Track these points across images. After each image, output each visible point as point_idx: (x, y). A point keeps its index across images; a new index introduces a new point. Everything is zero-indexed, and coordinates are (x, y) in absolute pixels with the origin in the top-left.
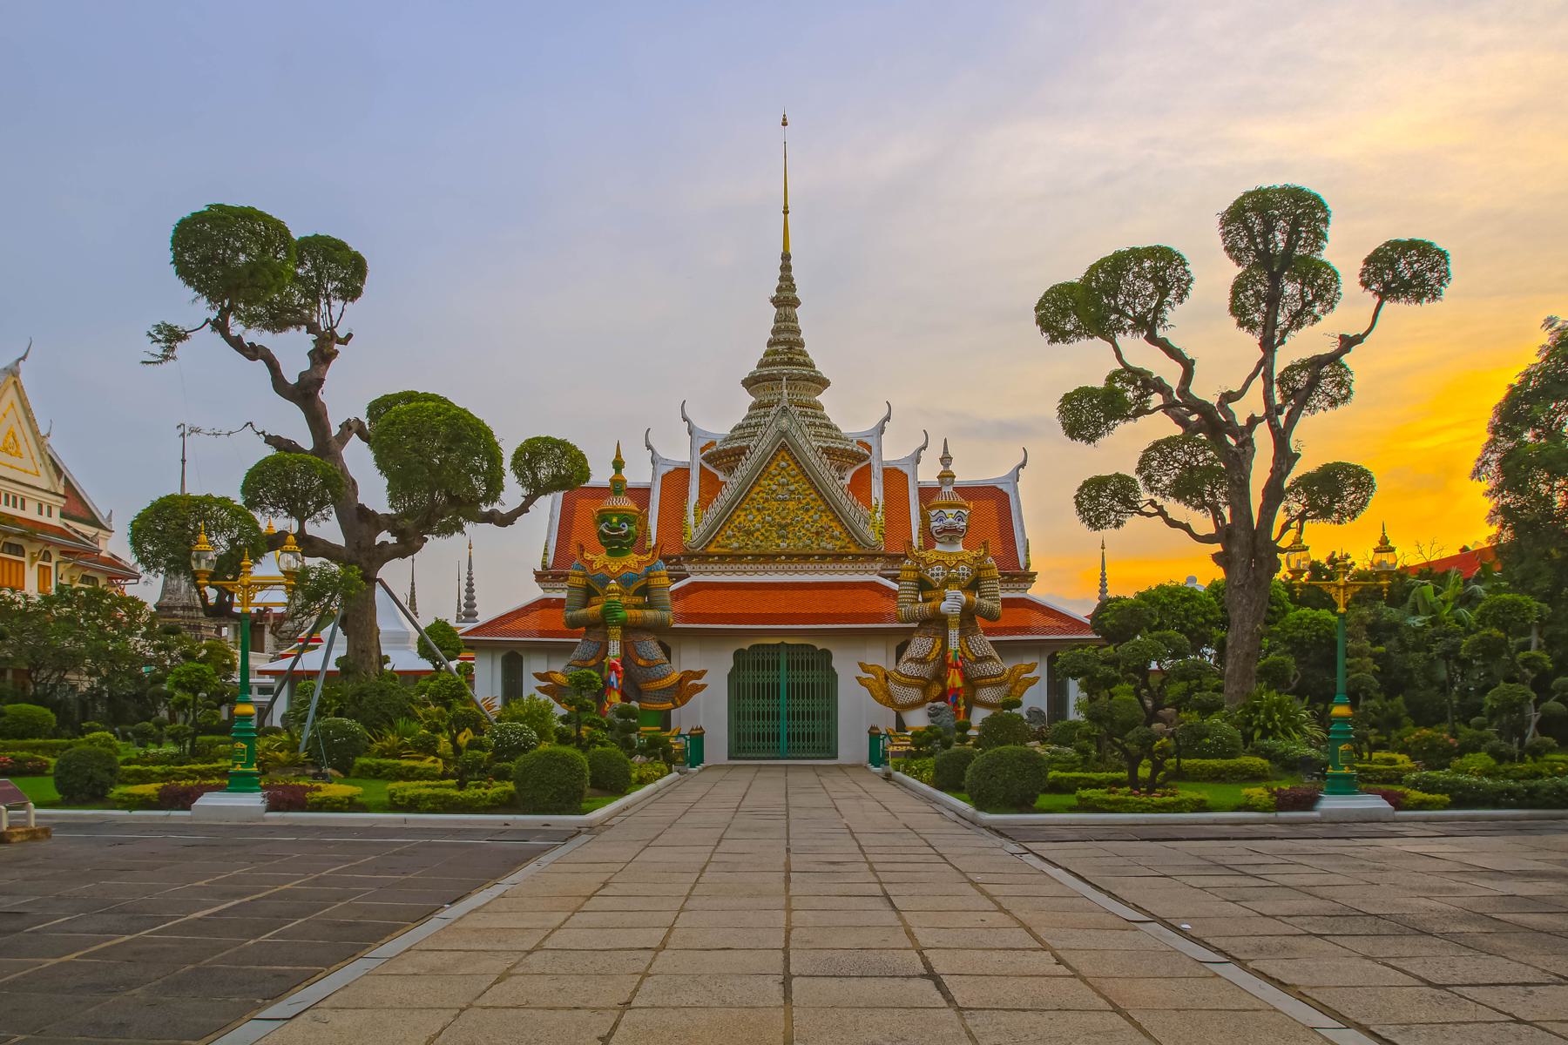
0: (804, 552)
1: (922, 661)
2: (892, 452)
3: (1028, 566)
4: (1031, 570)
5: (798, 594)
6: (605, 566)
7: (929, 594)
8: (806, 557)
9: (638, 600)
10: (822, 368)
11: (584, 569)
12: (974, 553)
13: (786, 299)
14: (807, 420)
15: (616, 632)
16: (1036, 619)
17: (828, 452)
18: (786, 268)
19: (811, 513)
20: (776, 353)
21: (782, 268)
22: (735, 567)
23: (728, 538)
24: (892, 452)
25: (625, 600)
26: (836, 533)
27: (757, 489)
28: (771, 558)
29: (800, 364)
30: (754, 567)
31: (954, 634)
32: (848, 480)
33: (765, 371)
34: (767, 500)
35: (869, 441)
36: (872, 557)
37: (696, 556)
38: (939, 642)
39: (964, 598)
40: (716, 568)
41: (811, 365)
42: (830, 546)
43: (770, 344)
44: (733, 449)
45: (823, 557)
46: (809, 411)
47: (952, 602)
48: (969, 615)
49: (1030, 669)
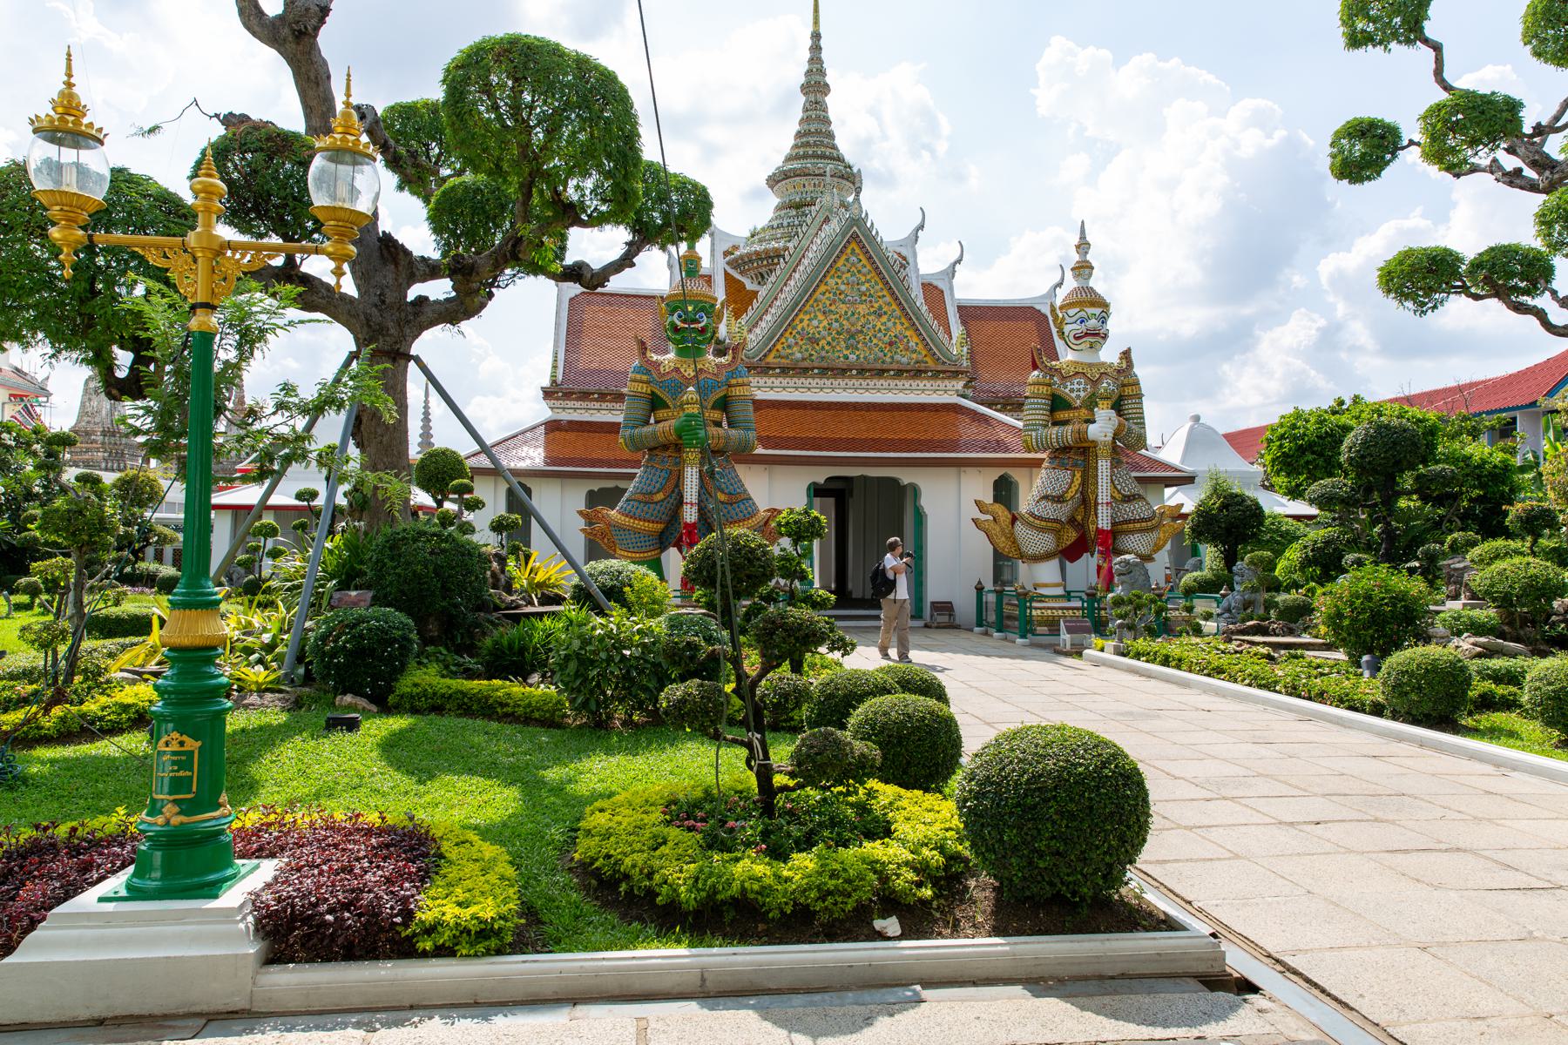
0: (878, 366)
1: (1059, 499)
2: (928, 263)
5: (874, 415)
6: (677, 370)
7: (1062, 415)
8: (881, 373)
9: (716, 415)
11: (648, 372)
13: (815, 86)
15: (692, 455)
18: (816, 48)
19: (884, 319)
20: (807, 144)
22: (799, 381)
24: (928, 263)
27: (823, 288)
28: (842, 372)
30: (821, 382)
31: (1104, 466)
33: (796, 165)
36: (955, 374)
38: (1078, 475)
40: (777, 382)
42: (904, 360)
43: (799, 135)
44: (766, 251)
45: (899, 373)
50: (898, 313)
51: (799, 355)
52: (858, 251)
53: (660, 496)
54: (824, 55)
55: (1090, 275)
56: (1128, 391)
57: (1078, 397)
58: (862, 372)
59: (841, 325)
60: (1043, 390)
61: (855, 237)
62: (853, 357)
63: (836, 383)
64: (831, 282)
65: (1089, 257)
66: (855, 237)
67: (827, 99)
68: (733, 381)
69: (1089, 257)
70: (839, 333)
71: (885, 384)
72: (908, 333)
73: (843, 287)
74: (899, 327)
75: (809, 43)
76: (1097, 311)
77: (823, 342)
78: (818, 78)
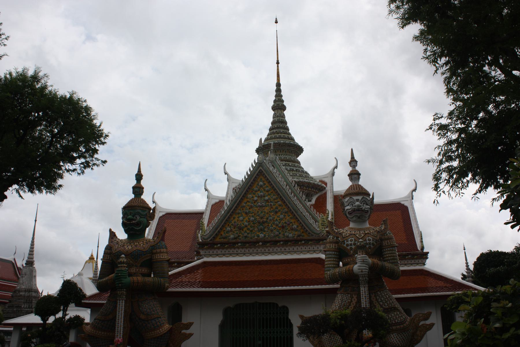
0: (274, 239)
3: (423, 248)
4: (425, 251)
9: (145, 270)
10: (299, 140)
12: (377, 229)
13: (279, 106)
14: (288, 168)
16: (432, 283)
17: (300, 184)
18: (278, 90)
19: (279, 214)
20: (273, 133)
21: (276, 91)
22: (231, 251)
25: (133, 270)
26: (295, 226)
27: (245, 200)
30: (243, 250)
31: (364, 290)
32: (313, 201)
34: (251, 207)
35: (326, 180)
38: (355, 297)
39: (370, 261)
40: (219, 252)
41: (293, 139)
42: (291, 235)
43: (271, 129)
46: (290, 164)
47: (360, 264)
48: (377, 276)
49: (427, 317)
50: (286, 210)
51: (232, 236)
52: (263, 179)
55: (359, 178)
56: (385, 243)
57: (351, 249)
60: (333, 246)
61: (261, 172)
62: (262, 235)
63: (251, 250)
64: (250, 196)
65: (357, 168)
66: (261, 172)
67: (285, 112)
68: (154, 251)
69: (357, 168)
70: (254, 224)
71: (279, 249)
72: (292, 221)
73: (256, 198)
74: (288, 218)
75: (275, 88)
76: (360, 198)
77: (245, 229)
78: (278, 103)
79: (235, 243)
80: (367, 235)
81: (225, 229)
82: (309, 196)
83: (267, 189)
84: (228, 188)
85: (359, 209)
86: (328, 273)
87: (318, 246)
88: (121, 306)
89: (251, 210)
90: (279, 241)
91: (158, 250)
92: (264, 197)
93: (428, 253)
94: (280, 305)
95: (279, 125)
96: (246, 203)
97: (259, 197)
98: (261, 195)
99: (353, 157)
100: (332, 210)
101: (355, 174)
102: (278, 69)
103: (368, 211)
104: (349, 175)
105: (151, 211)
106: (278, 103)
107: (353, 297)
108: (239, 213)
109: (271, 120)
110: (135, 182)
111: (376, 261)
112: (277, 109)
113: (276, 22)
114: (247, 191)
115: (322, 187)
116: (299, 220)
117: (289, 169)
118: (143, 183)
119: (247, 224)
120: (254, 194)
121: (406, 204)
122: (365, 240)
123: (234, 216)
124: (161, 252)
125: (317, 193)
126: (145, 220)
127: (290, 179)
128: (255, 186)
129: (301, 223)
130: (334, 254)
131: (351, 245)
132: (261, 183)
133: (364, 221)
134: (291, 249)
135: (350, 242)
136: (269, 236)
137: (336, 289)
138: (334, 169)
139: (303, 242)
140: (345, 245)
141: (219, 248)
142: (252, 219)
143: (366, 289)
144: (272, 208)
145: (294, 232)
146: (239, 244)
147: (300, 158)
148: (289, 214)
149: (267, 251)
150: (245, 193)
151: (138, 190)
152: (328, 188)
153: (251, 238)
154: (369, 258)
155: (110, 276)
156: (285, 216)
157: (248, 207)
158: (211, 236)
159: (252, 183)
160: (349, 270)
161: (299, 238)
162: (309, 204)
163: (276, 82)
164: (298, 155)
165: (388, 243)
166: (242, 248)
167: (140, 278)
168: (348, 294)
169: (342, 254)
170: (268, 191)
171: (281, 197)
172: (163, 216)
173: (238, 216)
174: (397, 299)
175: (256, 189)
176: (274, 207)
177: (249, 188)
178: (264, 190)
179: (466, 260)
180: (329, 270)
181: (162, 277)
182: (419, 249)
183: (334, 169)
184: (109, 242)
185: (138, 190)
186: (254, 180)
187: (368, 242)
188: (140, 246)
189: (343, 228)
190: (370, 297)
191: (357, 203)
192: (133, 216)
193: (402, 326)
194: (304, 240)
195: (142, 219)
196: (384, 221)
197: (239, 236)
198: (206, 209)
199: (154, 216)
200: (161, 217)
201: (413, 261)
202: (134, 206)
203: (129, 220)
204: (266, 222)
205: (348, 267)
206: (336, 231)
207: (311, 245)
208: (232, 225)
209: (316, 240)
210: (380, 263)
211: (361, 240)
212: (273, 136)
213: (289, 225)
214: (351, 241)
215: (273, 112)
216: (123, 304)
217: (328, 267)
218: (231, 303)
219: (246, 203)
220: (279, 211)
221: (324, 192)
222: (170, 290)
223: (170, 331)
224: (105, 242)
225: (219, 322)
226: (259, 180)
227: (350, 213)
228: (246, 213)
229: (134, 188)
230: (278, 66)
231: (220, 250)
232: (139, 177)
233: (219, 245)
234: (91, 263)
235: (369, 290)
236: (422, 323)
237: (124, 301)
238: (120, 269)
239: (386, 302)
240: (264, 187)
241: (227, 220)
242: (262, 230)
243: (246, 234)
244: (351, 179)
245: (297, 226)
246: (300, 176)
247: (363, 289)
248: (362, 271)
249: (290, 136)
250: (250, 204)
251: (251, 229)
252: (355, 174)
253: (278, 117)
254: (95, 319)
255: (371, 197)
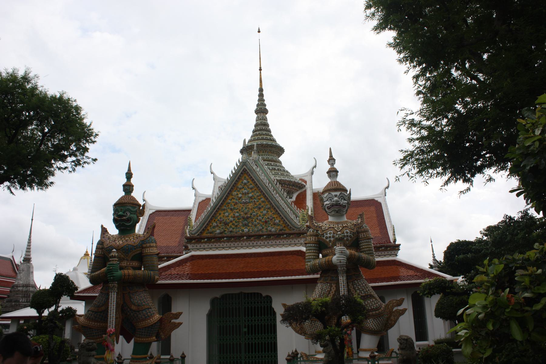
0: (258, 233)
4: (397, 243)
7: (325, 252)
8: (258, 237)
9: (135, 264)
10: (280, 142)
12: (354, 222)
13: (261, 110)
16: (403, 272)
17: (281, 182)
18: (261, 95)
19: (262, 210)
20: (257, 135)
23: (214, 227)
25: (124, 264)
26: (277, 221)
27: (230, 197)
29: (268, 140)
31: (342, 279)
32: (294, 198)
34: (236, 203)
35: (305, 178)
37: (194, 239)
38: (334, 286)
39: (348, 252)
40: (206, 246)
41: (274, 140)
42: (273, 230)
43: (254, 132)
46: (272, 163)
48: (354, 266)
49: (400, 303)
50: (269, 206)
51: (218, 231)
52: (247, 178)
53: (103, 308)
54: (264, 98)
55: (337, 175)
56: (362, 235)
57: (330, 241)
58: (249, 237)
59: (240, 215)
60: (313, 239)
61: (245, 170)
62: (246, 230)
63: (236, 244)
65: (335, 166)
66: (245, 170)
67: (267, 116)
68: (145, 246)
69: (335, 166)
71: (262, 243)
72: (275, 216)
73: (240, 195)
74: (270, 213)
75: (258, 93)
76: (338, 193)
78: (260, 107)
79: (221, 238)
80: (345, 228)
81: (211, 224)
82: (290, 194)
83: (251, 186)
84: (214, 187)
85: (337, 204)
86: (309, 264)
87: (299, 239)
88: (113, 298)
89: (236, 206)
90: (263, 235)
91: (148, 245)
92: (248, 194)
93: (399, 245)
94: (264, 295)
95: (262, 127)
96: (231, 200)
97: (243, 194)
98: (245, 193)
99: (331, 156)
100: (312, 206)
101: (333, 171)
102: (260, 76)
103: (345, 206)
104: (328, 173)
105: (141, 208)
106: (260, 107)
107: (331, 286)
108: (224, 210)
109: (254, 122)
110: (125, 181)
111: (353, 252)
112: (259, 112)
113: (259, 32)
114: (232, 188)
115: (302, 185)
116: (280, 216)
117: (271, 168)
118: (133, 181)
119: (232, 219)
120: (239, 191)
121: (380, 200)
122: (343, 233)
123: (220, 212)
124: (150, 247)
125: (297, 191)
126: (135, 216)
127: (272, 177)
128: (240, 183)
129: (282, 218)
130: (314, 247)
131: (330, 237)
132: (245, 181)
133: (342, 215)
134: (274, 242)
135: (329, 235)
136: (253, 230)
137: (317, 279)
138: (313, 168)
139: (285, 236)
140: (324, 238)
141: (205, 243)
142: (237, 214)
143: (344, 278)
144: (256, 204)
145: (276, 227)
146: (225, 239)
147: (281, 158)
148: (272, 210)
149: (251, 244)
150: (230, 191)
151: (128, 188)
152: (308, 186)
153: (236, 233)
154: (347, 249)
155: (102, 270)
156: (267, 211)
157: (233, 204)
158: (198, 231)
159: (237, 181)
160: (328, 261)
161: (281, 232)
162: (290, 200)
163: (259, 87)
164: (279, 155)
165: (364, 235)
166: (228, 242)
167: (131, 272)
168: (328, 283)
169: (321, 246)
170: (251, 189)
171: (264, 194)
172: (153, 213)
173: (223, 212)
174: (373, 287)
175: (240, 186)
176: (257, 203)
177: (233, 186)
178: (248, 187)
179: (433, 252)
180: (310, 262)
181: (151, 270)
182: (392, 241)
183: (313, 168)
184: (101, 238)
185: (128, 188)
186: (238, 178)
187: (346, 234)
188: (131, 240)
189: (322, 221)
190: (348, 286)
191: (336, 199)
192: (124, 213)
193: (377, 312)
194: (286, 234)
195: (132, 215)
196: (360, 215)
197: (225, 231)
198: (194, 207)
199: (144, 212)
200: (151, 214)
201: (386, 253)
202: (125, 203)
203: (120, 216)
204: (250, 217)
205: (327, 258)
206: (316, 225)
207: (292, 238)
208: (218, 220)
209: (297, 234)
210: (356, 254)
211: (339, 233)
212: (256, 137)
213: (271, 220)
214: (330, 234)
215: (256, 116)
216: (115, 295)
217: (310, 259)
218: (218, 294)
219: (231, 200)
220: (262, 207)
221: (304, 190)
222: (159, 282)
223: (161, 320)
224: (97, 238)
225: (207, 312)
226: (243, 178)
227: (329, 208)
228: (231, 209)
229: (124, 186)
230: (260, 73)
231: (207, 244)
232: (129, 175)
233: (206, 240)
234: (86, 259)
235: (347, 279)
236: (395, 309)
237: (115, 293)
238: (111, 263)
239: (363, 290)
240: (248, 184)
241: (213, 216)
242: (246, 225)
243: (231, 229)
244: (330, 177)
245: (280, 221)
246: (282, 175)
247: (342, 278)
248: (340, 262)
249: (272, 138)
250: (235, 201)
251: (236, 224)
252: (333, 171)
253: (260, 120)
254: (88, 311)
255: (348, 193)
